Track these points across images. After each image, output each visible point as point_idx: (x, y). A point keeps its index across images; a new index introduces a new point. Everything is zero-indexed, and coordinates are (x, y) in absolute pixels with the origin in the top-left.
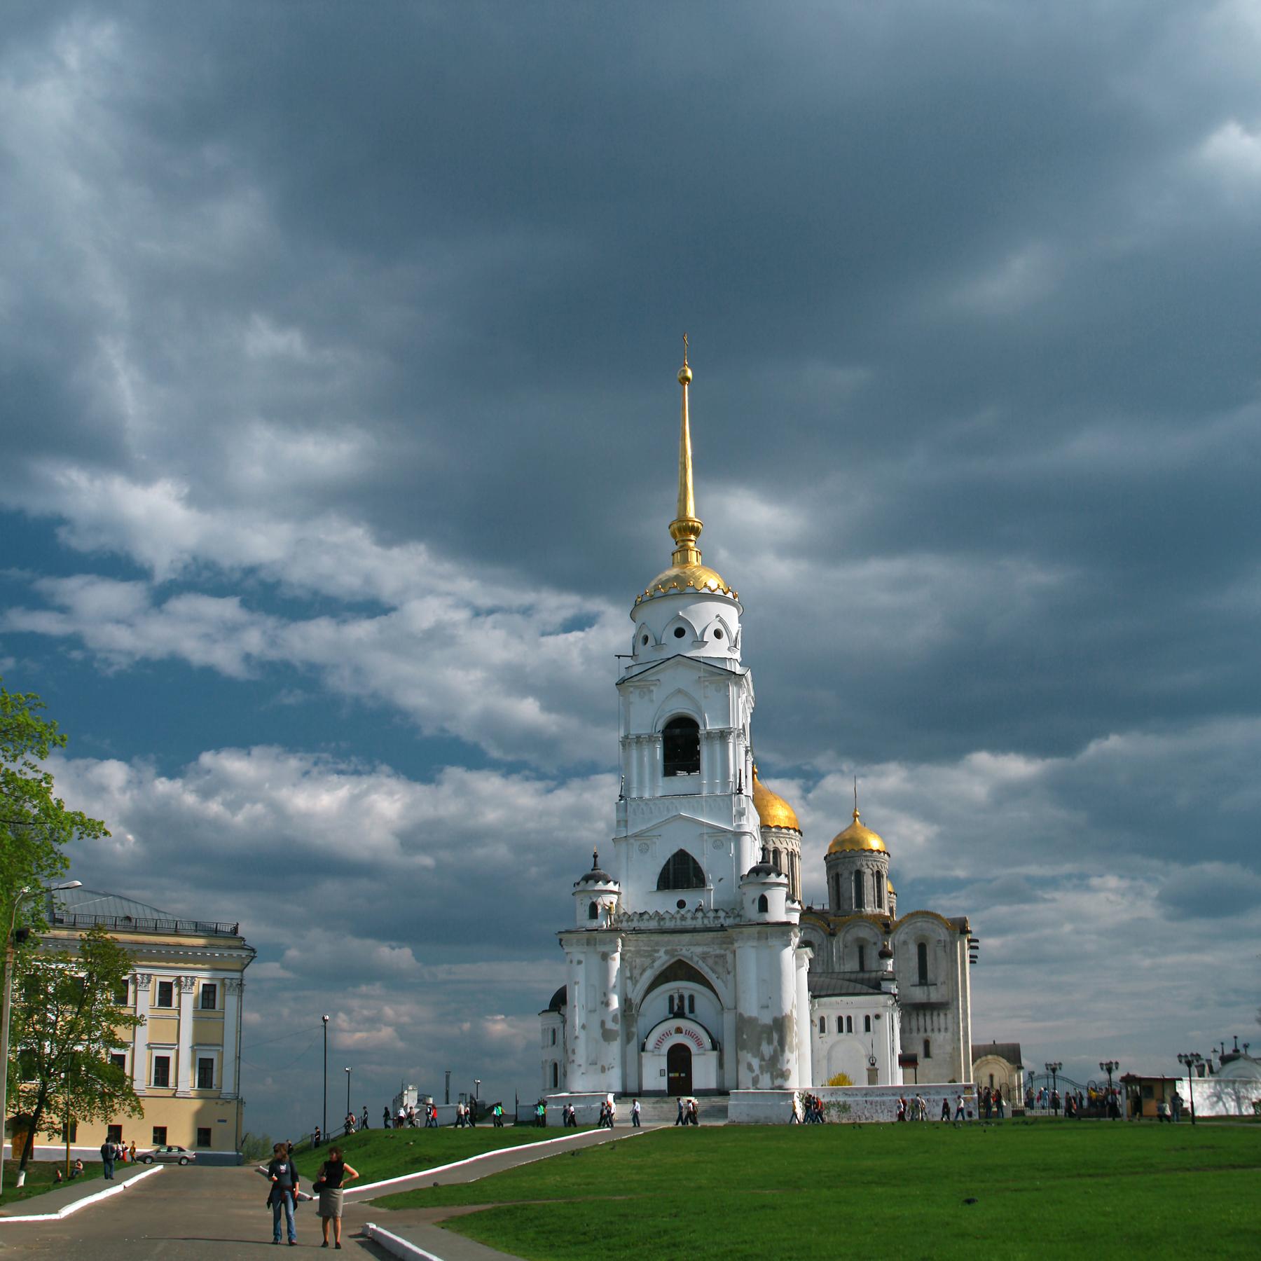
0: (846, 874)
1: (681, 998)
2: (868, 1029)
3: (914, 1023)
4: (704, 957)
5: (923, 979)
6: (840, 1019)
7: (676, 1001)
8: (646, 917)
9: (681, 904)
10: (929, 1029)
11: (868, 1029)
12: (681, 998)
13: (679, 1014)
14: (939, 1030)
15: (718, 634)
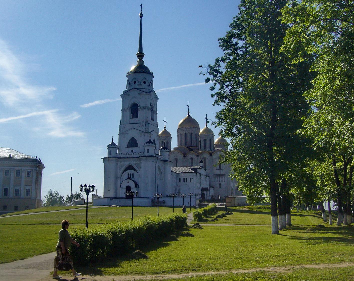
0: (202, 140)
1: (131, 174)
2: (190, 181)
3: (217, 179)
4: (136, 164)
5: (220, 168)
6: (184, 178)
7: (130, 175)
8: (123, 154)
9: (132, 151)
10: (220, 181)
11: (190, 181)
12: (131, 174)
13: (129, 178)
14: (223, 181)
15: (145, 83)
